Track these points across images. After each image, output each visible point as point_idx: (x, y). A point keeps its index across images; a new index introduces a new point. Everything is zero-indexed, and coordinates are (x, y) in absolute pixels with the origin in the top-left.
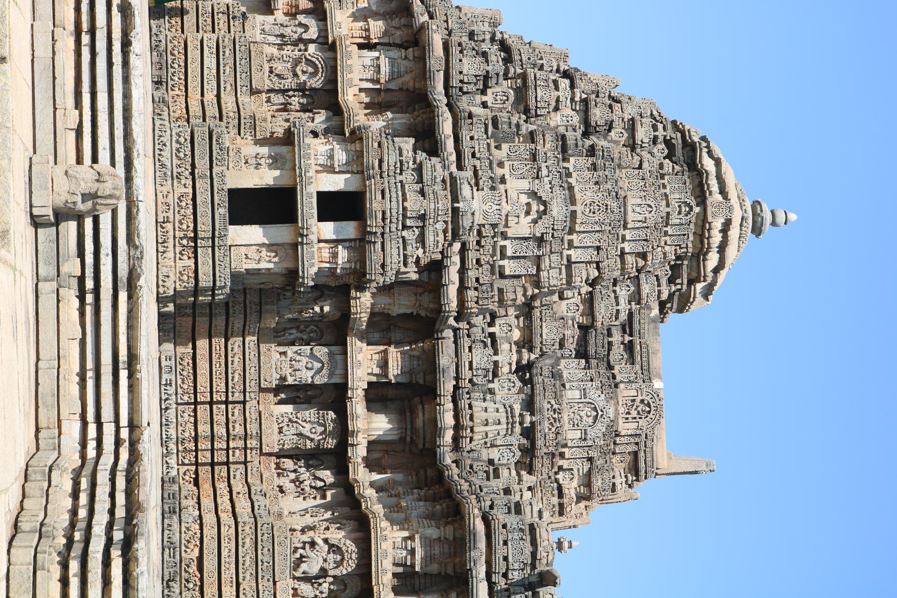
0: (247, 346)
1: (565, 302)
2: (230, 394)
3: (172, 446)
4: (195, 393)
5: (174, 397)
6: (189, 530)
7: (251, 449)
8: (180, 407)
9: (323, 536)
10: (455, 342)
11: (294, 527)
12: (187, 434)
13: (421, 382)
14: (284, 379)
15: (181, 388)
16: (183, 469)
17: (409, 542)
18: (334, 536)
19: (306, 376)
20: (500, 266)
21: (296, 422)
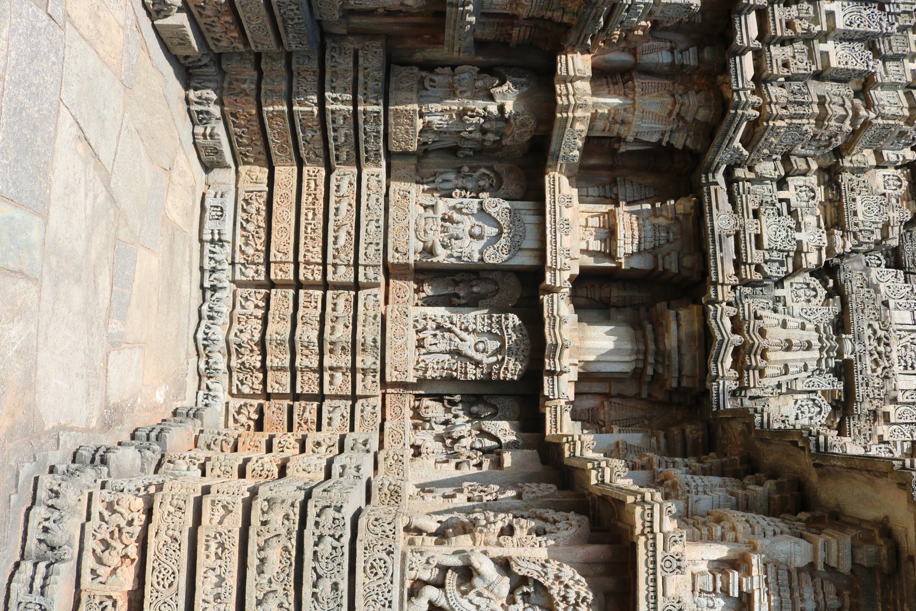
1: (881, 172)
2: (330, 269)
6: (114, 512)
7: (365, 372)
9: (496, 552)
10: (732, 200)
11: (416, 522)
12: (245, 337)
13: (674, 269)
14: (429, 251)
15: (243, 252)
16: (236, 403)
17: (735, 576)
18: (526, 552)
19: (470, 250)
20: (822, 53)
21: (450, 330)
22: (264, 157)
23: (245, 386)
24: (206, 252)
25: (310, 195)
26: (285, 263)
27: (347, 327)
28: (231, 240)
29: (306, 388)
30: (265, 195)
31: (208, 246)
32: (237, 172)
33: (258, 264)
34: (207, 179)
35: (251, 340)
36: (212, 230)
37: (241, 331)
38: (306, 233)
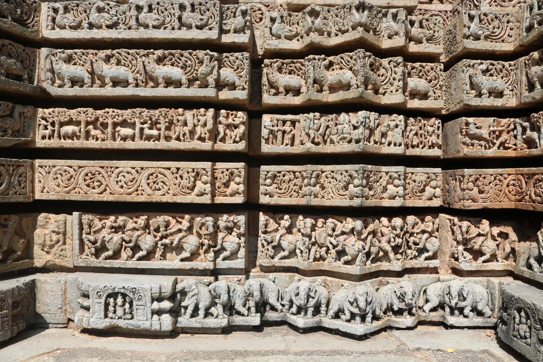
0: (68, 34)
2: (225, 95)
3: (387, 292)
4: (215, 209)
5: (222, 283)
8: (262, 260)
12: (353, 245)
15: (194, 255)
22: (14, 219)
23: (428, 246)
24: (195, 323)
25: (88, 133)
26: (214, 178)
27: (331, 64)
28: (172, 278)
29: (434, 139)
30: (86, 218)
31: (184, 321)
32: (46, 269)
33: (216, 227)
34: (57, 325)
35: (360, 233)
36: (153, 313)
37: (341, 253)
38: (158, 138)
